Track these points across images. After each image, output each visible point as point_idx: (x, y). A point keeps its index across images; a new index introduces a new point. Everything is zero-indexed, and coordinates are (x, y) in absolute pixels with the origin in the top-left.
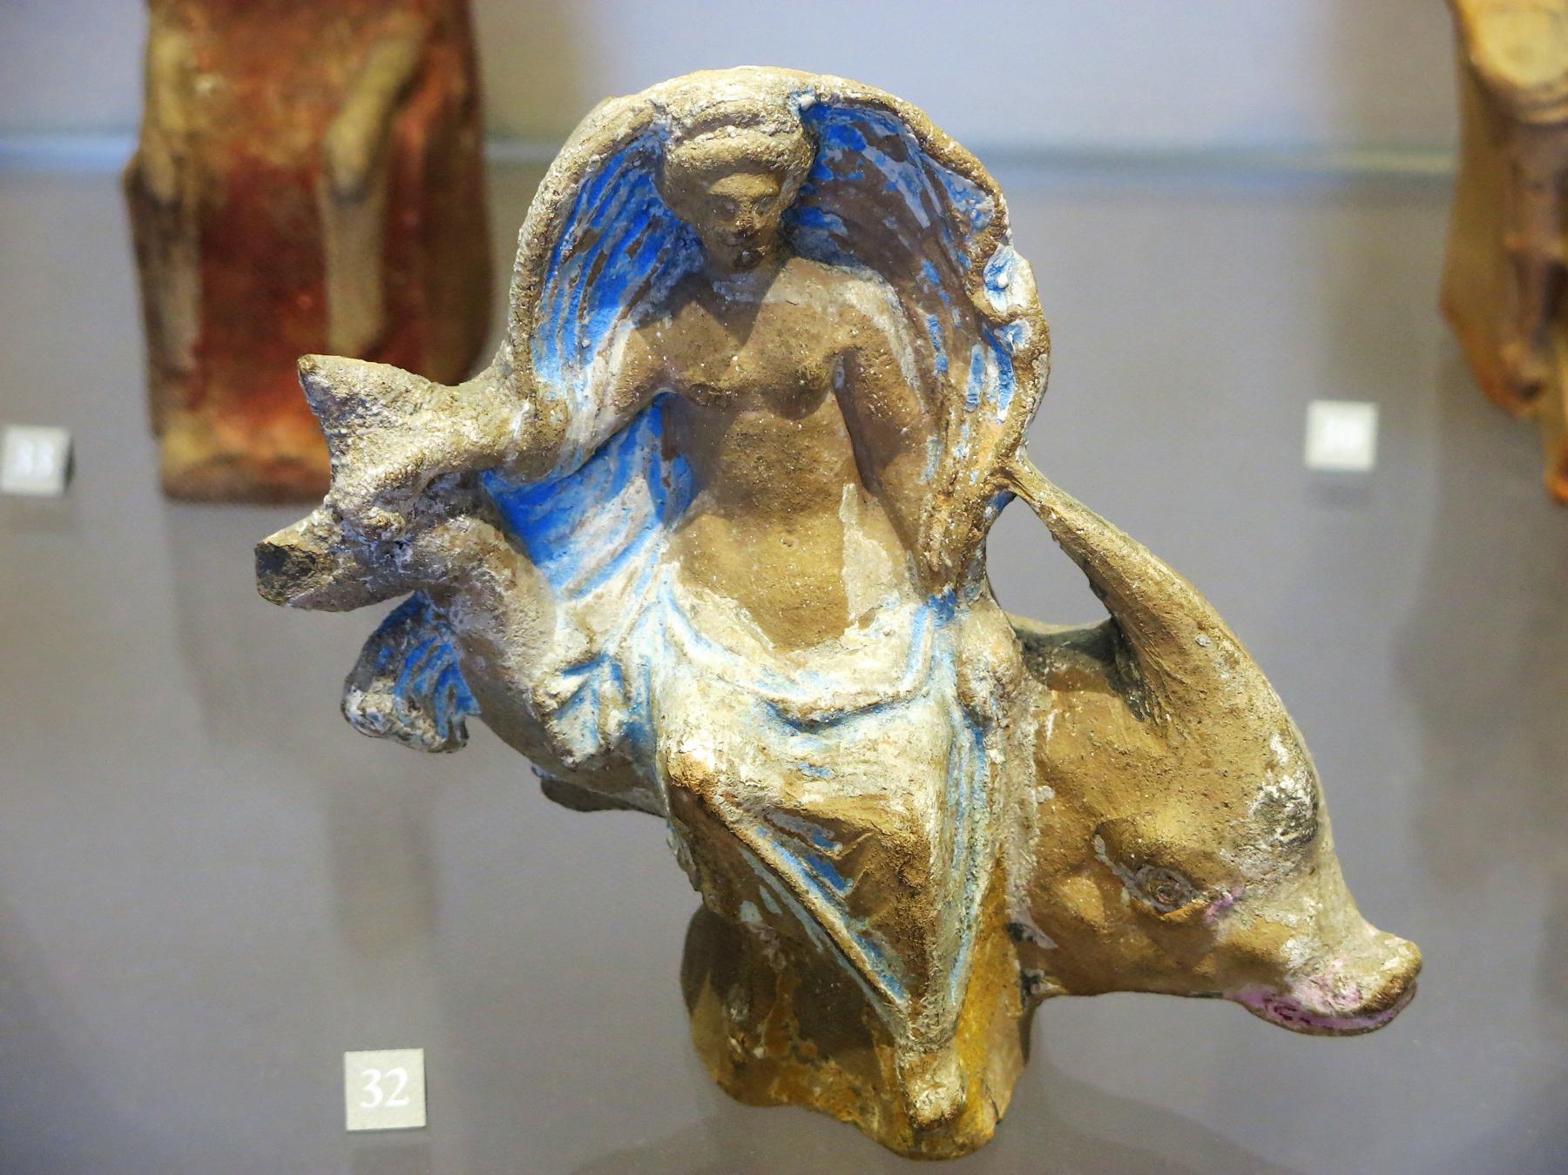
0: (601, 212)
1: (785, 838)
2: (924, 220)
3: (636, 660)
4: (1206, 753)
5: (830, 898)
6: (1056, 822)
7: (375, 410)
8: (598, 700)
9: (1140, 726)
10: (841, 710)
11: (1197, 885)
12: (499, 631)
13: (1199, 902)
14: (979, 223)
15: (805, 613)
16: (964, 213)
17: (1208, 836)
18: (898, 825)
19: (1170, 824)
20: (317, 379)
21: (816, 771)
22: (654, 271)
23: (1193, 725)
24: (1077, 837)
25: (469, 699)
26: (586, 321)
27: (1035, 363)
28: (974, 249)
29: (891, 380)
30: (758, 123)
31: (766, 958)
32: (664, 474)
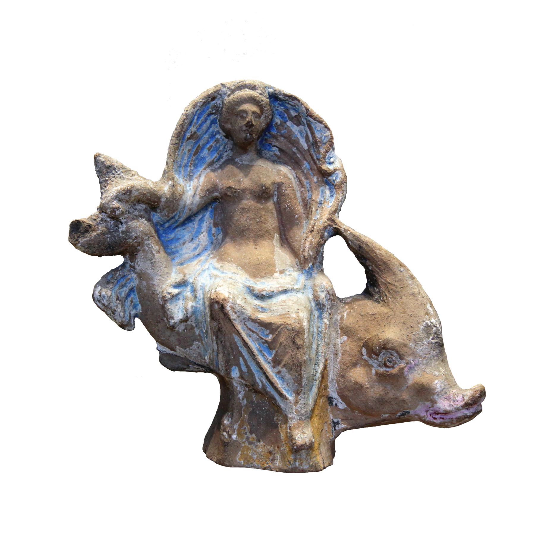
0: (201, 126)
1: (251, 333)
2: (305, 146)
3: (200, 284)
4: (404, 309)
5: (266, 360)
6: (348, 348)
7: (119, 172)
8: (185, 298)
9: (379, 305)
10: (273, 292)
11: (401, 357)
12: (152, 269)
13: (402, 365)
14: (325, 141)
15: (261, 266)
16: (320, 138)
17: (405, 338)
18: (293, 321)
19: (392, 334)
20: (100, 158)
21: (263, 310)
22: (216, 157)
23: (399, 299)
24: (356, 350)
25: (138, 305)
26: (192, 168)
27: (342, 186)
28: (322, 150)
29: (293, 197)
30: (255, 89)
31: (239, 399)
32: (213, 232)
